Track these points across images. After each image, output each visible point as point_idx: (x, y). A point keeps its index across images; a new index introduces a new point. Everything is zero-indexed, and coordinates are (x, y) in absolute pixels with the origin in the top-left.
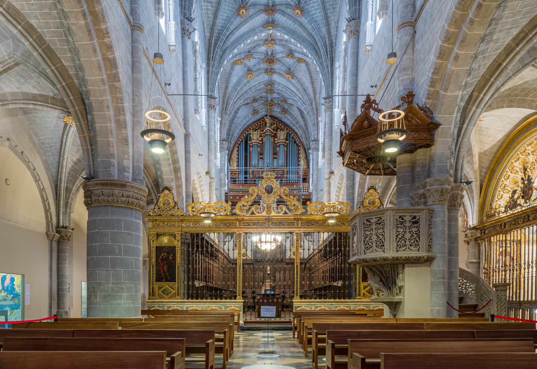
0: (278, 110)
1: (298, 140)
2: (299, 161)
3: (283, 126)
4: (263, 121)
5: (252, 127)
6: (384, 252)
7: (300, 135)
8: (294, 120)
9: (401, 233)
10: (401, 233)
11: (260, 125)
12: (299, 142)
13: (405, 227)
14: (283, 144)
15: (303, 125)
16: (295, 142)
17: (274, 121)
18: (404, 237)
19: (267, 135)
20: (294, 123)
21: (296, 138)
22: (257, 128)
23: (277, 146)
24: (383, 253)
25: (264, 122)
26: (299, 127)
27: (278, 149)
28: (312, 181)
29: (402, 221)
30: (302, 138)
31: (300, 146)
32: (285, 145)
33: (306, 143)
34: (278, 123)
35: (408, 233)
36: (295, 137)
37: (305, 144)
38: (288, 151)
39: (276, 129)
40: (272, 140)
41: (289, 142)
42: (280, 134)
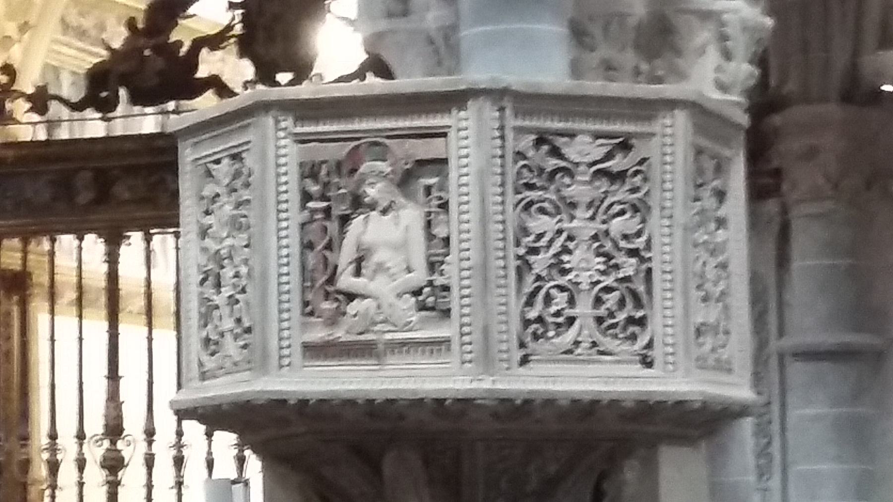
6: (647, 363)
24: (637, 369)
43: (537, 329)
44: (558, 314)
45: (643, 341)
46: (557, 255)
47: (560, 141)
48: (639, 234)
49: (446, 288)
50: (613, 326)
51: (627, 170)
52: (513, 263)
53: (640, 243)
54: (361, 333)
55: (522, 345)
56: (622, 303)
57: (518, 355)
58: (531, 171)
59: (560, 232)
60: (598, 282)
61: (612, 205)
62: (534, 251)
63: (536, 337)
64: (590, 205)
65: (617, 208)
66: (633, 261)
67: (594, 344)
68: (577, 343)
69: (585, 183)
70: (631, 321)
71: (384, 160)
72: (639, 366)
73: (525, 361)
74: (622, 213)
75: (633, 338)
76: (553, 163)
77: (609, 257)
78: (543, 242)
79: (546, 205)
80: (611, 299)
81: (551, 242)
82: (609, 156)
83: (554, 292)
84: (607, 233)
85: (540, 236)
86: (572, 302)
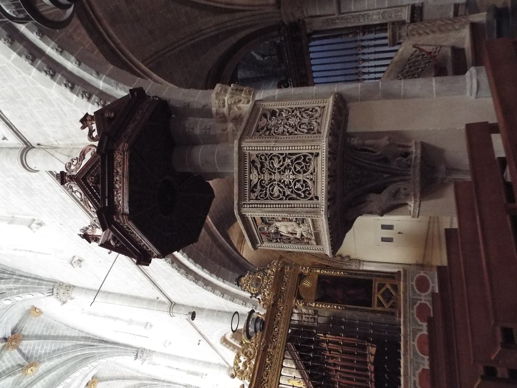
6: (317, 155)
9: (285, 129)
10: (285, 129)
13: (276, 126)
18: (295, 125)
24: (319, 158)
29: (265, 129)
35: (289, 121)
43: (307, 193)
44: (302, 186)
45: (311, 157)
46: (285, 187)
47: (253, 185)
48: (279, 158)
49: (296, 219)
50: (306, 166)
51: (260, 161)
52: (288, 201)
53: (281, 157)
54: (312, 235)
55: (312, 199)
56: (299, 164)
57: (315, 201)
58: (261, 194)
59: (278, 185)
60: (293, 172)
61: (270, 166)
62: (284, 192)
63: (310, 194)
64: (271, 174)
65: (271, 165)
66: (287, 159)
67: (312, 174)
68: (311, 180)
69: (264, 176)
70: (304, 160)
71: (264, 228)
72: (318, 158)
73: (317, 198)
74: (272, 163)
75: (310, 159)
76: (259, 187)
77: (285, 168)
78: (281, 190)
79: (271, 189)
80: (298, 168)
81: (281, 187)
82: (256, 168)
83: (296, 188)
84: (279, 169)
85: (280, 192)
86: (299, 181)
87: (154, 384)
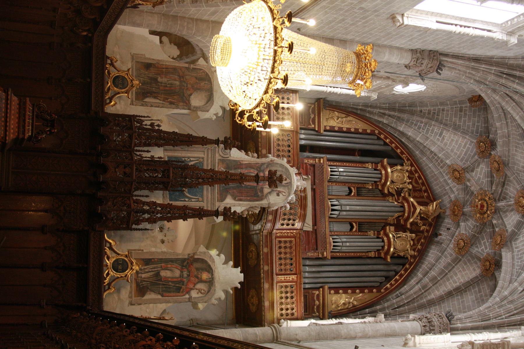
0: (463, 232)
1: (392, 285)
2: (345, 290)
3: (419, 247)
4: (428, 197)
5: (416, 171)
7: (403, 290)
8: (440, 274)
11: (420, 190)
12: (387, 289)
14: (383, 247)
15: (429, 298)
16: (388, 279)
17: (430, 225)
19: (403, 207)
20: (433, 273)
21: (396, 281)
22: (414, 184)
23: (379, 233)
25: (425, 200)
26: (424, 287)
27: (371, 233)
28: (322, 325)
30: (397, 297)
31: (379, 291)
32: (379, 254)
33: (388, 307)
34: (426, 234)
36: (397, 277)
37: (386, 305)
38: (369, 261)
39: (414, 229)
40: (390, 220)
41: (387, 264)
42: (405, 239)
87: (517, 314)
